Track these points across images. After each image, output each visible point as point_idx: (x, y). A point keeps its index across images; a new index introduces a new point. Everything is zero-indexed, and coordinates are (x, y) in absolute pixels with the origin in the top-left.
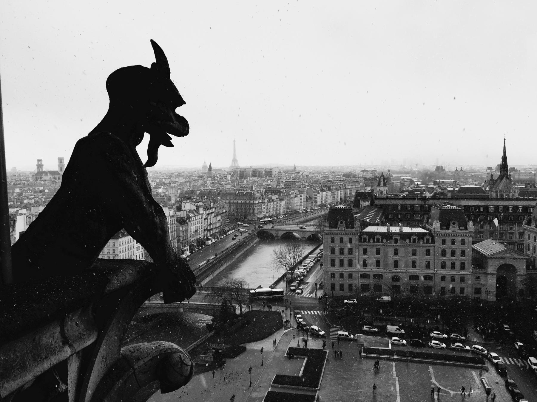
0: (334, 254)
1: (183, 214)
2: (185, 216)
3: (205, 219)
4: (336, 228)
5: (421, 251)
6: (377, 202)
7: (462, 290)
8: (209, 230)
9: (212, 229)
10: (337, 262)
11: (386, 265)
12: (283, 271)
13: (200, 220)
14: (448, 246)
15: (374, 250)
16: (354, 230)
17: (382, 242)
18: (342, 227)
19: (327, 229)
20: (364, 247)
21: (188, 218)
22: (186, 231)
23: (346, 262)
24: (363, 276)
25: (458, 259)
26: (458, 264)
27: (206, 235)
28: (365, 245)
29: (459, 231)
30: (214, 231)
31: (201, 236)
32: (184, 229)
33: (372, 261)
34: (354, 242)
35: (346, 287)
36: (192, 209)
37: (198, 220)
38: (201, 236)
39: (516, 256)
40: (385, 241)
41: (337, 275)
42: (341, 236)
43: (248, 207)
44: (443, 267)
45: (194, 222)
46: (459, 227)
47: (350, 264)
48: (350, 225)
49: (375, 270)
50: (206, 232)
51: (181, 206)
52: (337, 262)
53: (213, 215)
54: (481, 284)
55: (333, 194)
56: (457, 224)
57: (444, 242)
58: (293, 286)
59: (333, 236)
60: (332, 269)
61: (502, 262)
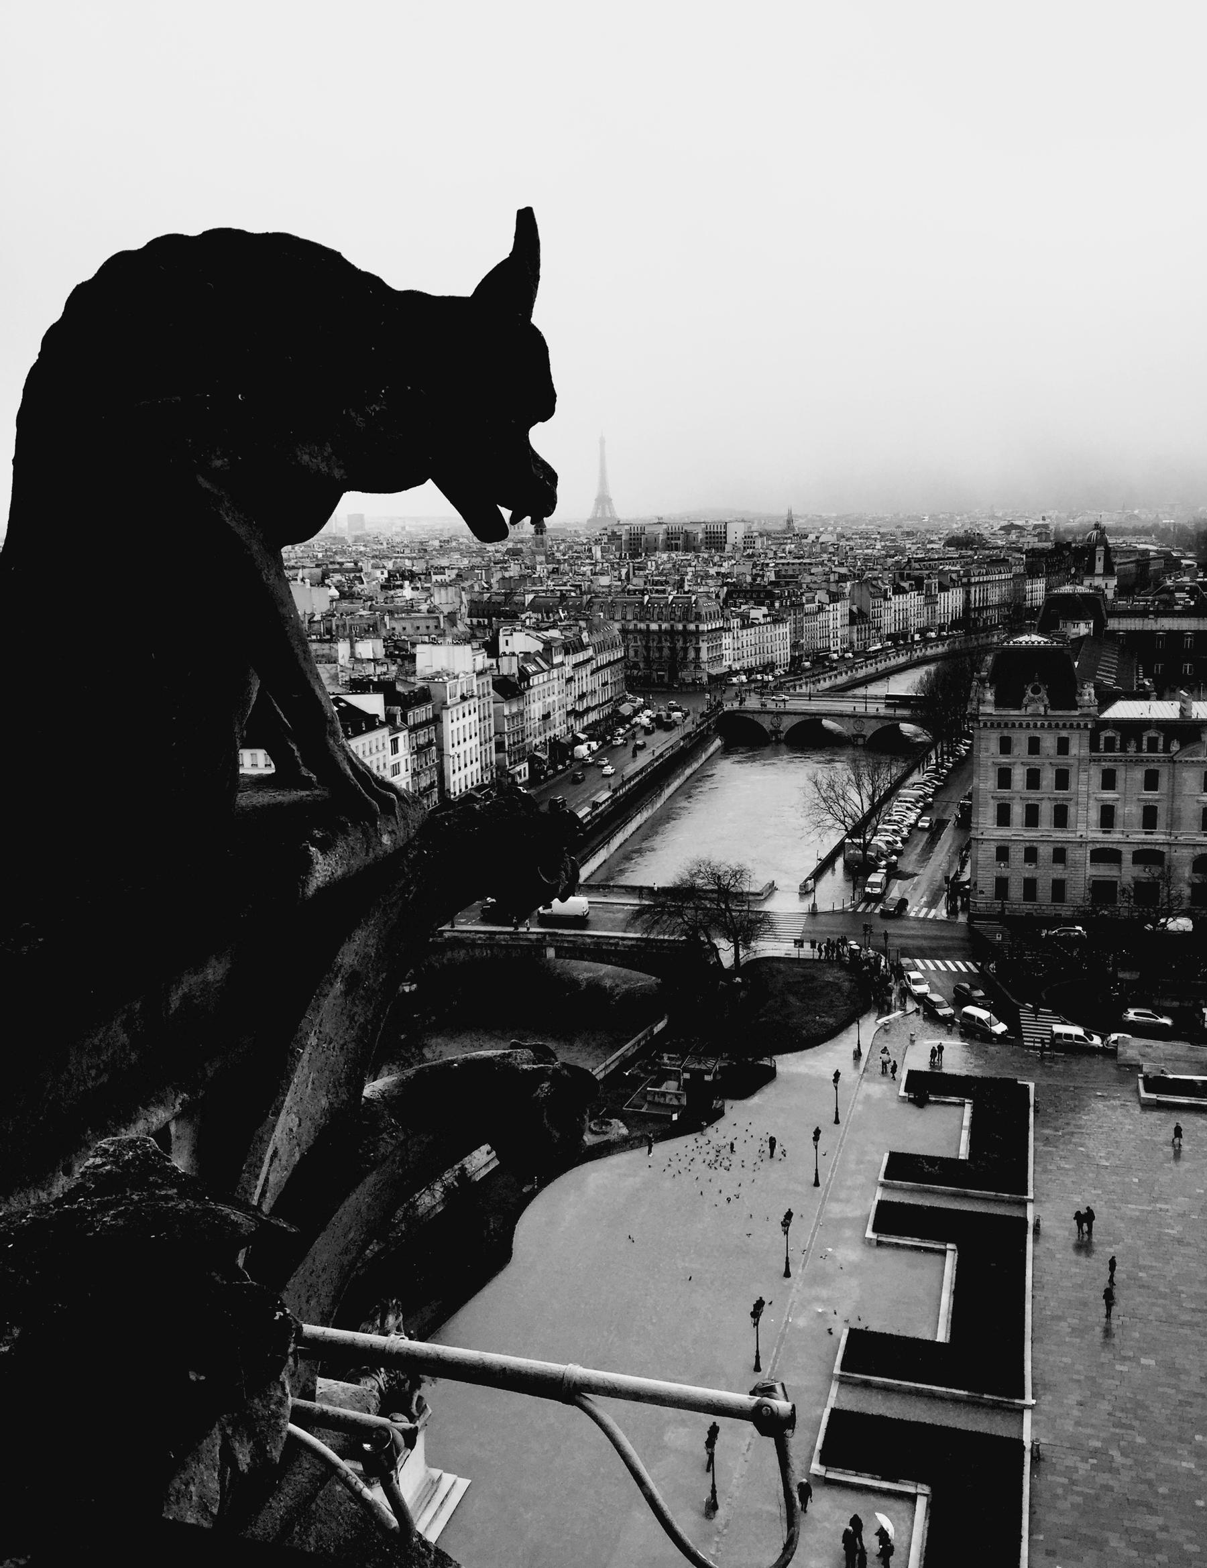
1: (509, 667)
2: (515, 670)
3: (570, 680)
6: (1113, 624)
8: (578, 715)
9: (588, 710)
12: (833, 839)
13: (556, 683)
15: (1139, 775)
16: (1077, 713)
17: (1166, 749)
18: (1036, 705)
19: (989, 709)
21: (524, 676)
22: (521, 714)
23: (1046, 812)
27: (570, 729)
30: (593, 717)
31: (558, 730)
32: (514, 710)
33: (1129, 811)
34: (1074, 751)
35: (1044, 891)
37: (550, 684)
40: (1175, 747)
43: (680, 644)
45: (540, 689)
47: (1061, 818)
48: (1064, 697)
49: (1100, 836)
50: (571, 721)
53: (589, 668)
55: (931, 601)
58: (873, 885)
59: (1006, 733)
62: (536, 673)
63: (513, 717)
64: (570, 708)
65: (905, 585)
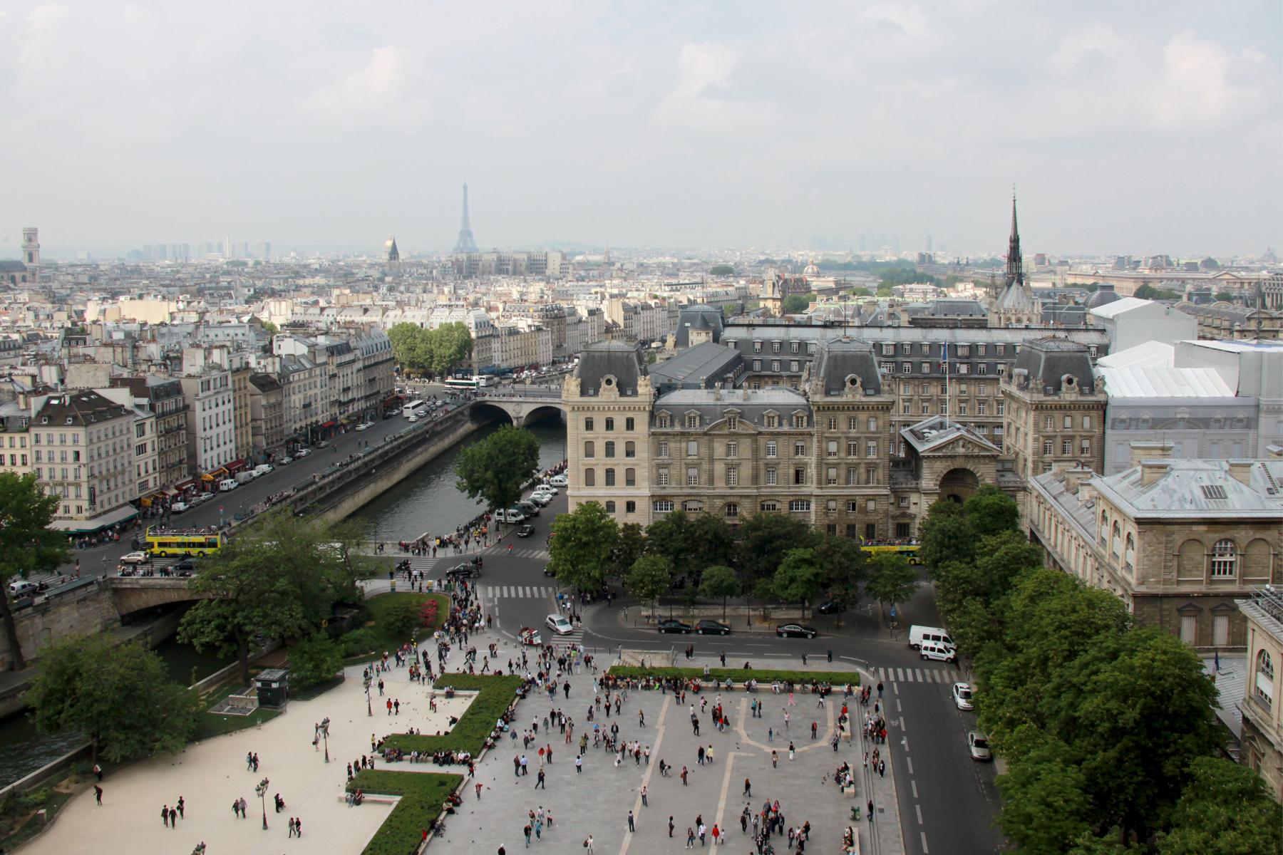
0: (592, 456)
1: (271, 367)
2: (278, 368)
3: (334, 376)
8: (340, 404)
9: (352, 401)
18: (609, 394)
31: (322, 418)
32: (272, 400)
36: (298, 354)
38: (319, 418)
42: (609, 415)
45: (302, 384)
47: (630, 481)
48: (626, 387)
50: (336, 410)
51: (271, 343)
52: (600, 476)
59: (589, 415)
64: (332, 399)
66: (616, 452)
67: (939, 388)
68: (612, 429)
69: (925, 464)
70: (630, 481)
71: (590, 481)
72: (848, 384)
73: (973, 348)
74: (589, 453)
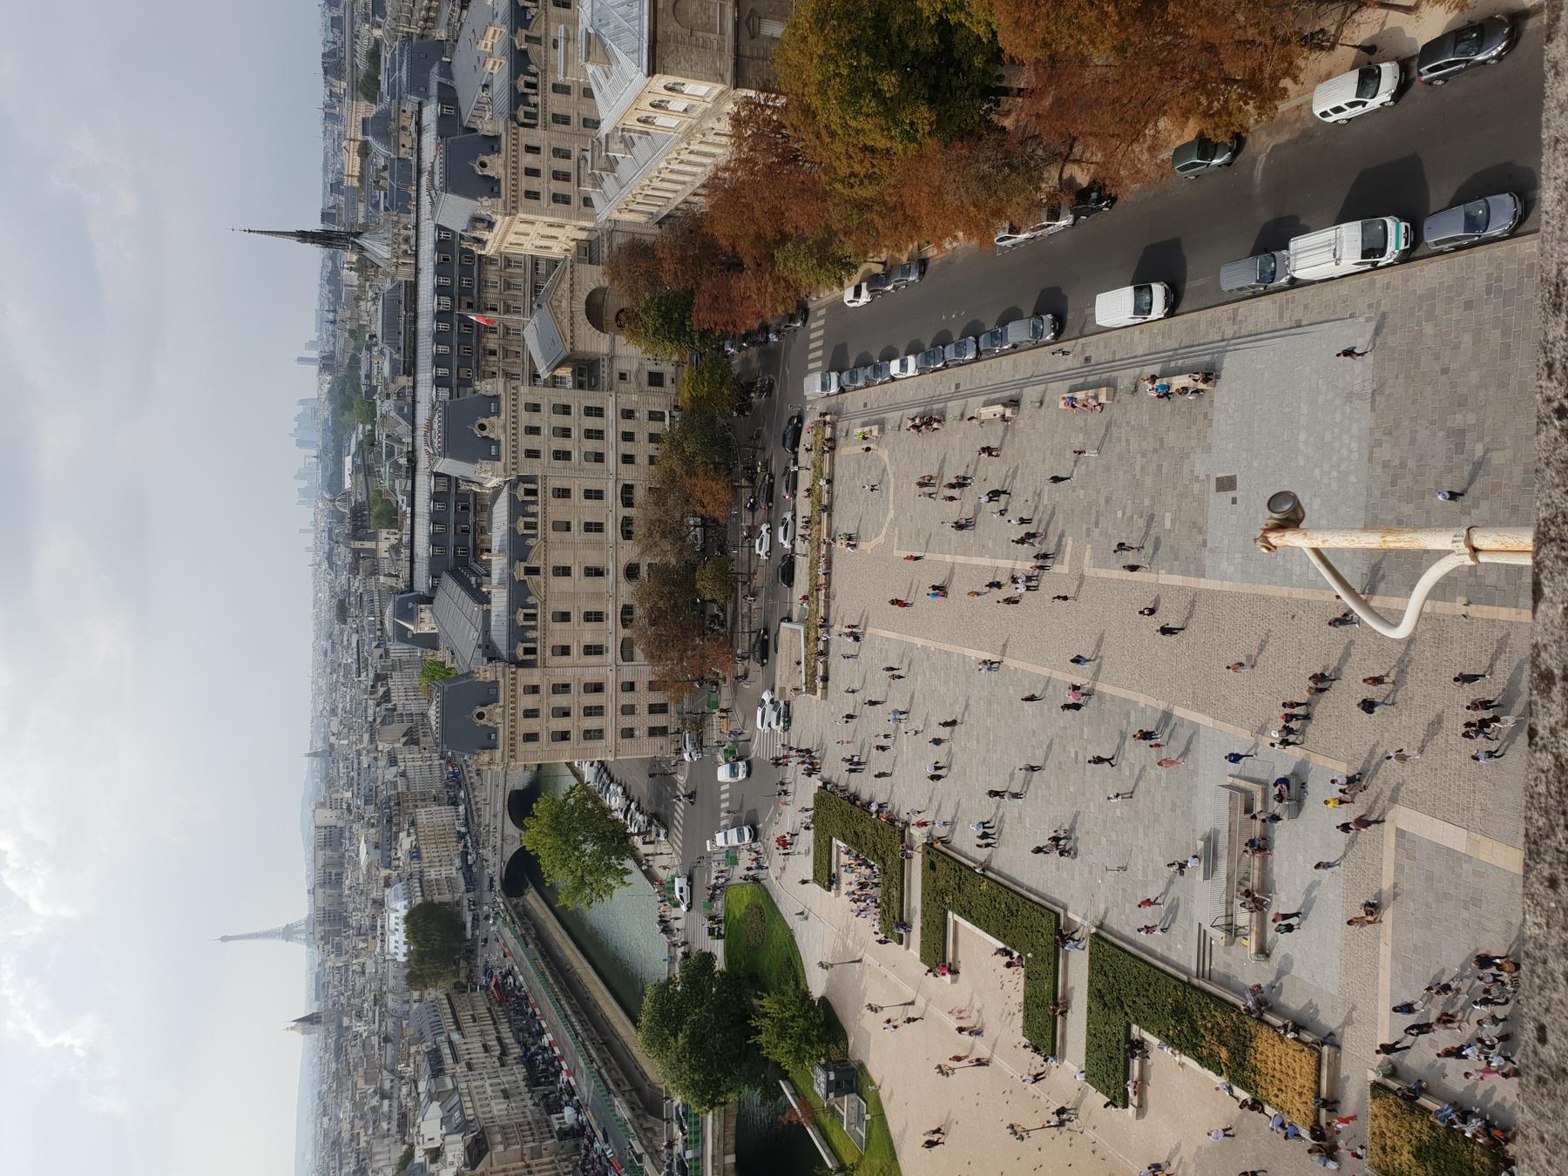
2: (458, 1137)
3: (470, 1067)
4: (495, 731)
5: (558, 510)
7: (655, 416)
8: (504, 1053)
9: (499, 1039)
10: (592, 723)
11: (597, 596)
14: (546, 443)
15: (558, 626)
16: (501, 680)
18: (496, 715)
19: (498, 754)
20: (549, 653)
23: (593, 700)
24: (626, 652)
25: (578, 422)
26: (592, 423)
28: (545, 652)
29: (503, 416)
31: (519, 1072)
32: (498, 1138)
38: (520, 1077)
39: (565, 286)
41: (628, 722)
42: (520, 714)
44: (599, 458)
46: (493, 414)
47: (598, 688)
48: (489, 694)
50: (510, 1059)
52: (592, 723)
54: (638, 371)
56: (484, 421)
57: (533, 454)
59: (520, 738)
60: (610, 735)
61: (581, 317)
62: (462, 1112)
63: (506, 1142)
65: (381, 691)
66: (565, 704)
67: (491, 336)
68: (537, 710)
69: (580, 347)
70: (598, 688)
71: (598, 734)
72: (485, 433)
73: (440, 290)
74: (564, 736)
